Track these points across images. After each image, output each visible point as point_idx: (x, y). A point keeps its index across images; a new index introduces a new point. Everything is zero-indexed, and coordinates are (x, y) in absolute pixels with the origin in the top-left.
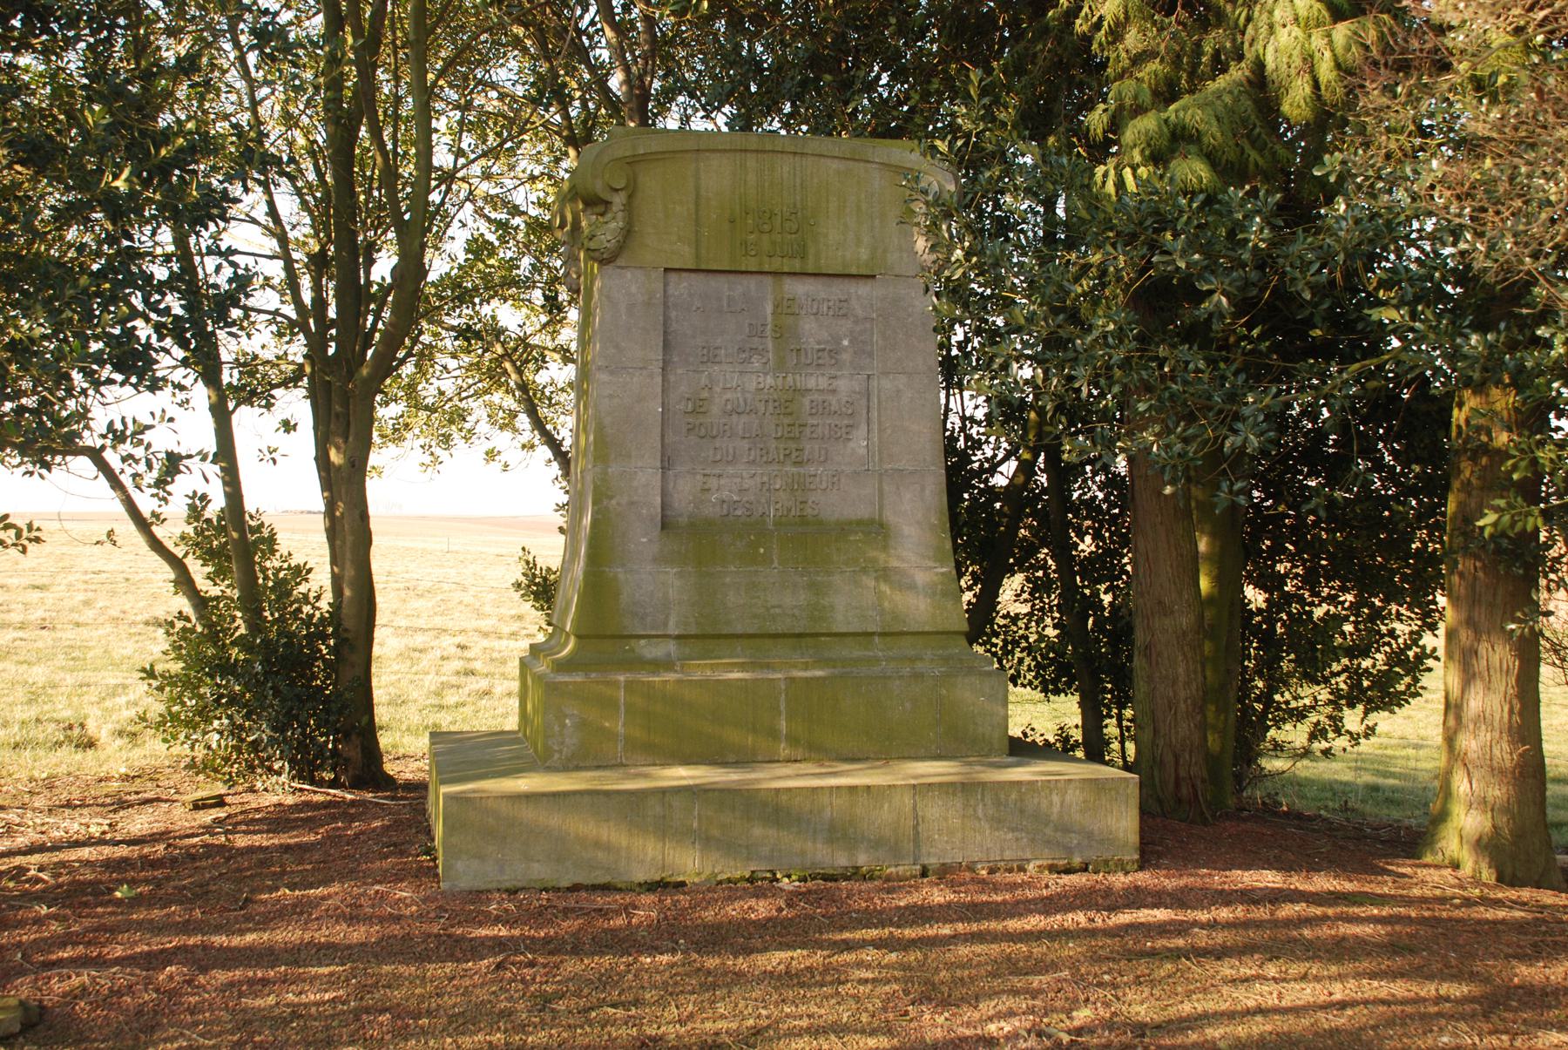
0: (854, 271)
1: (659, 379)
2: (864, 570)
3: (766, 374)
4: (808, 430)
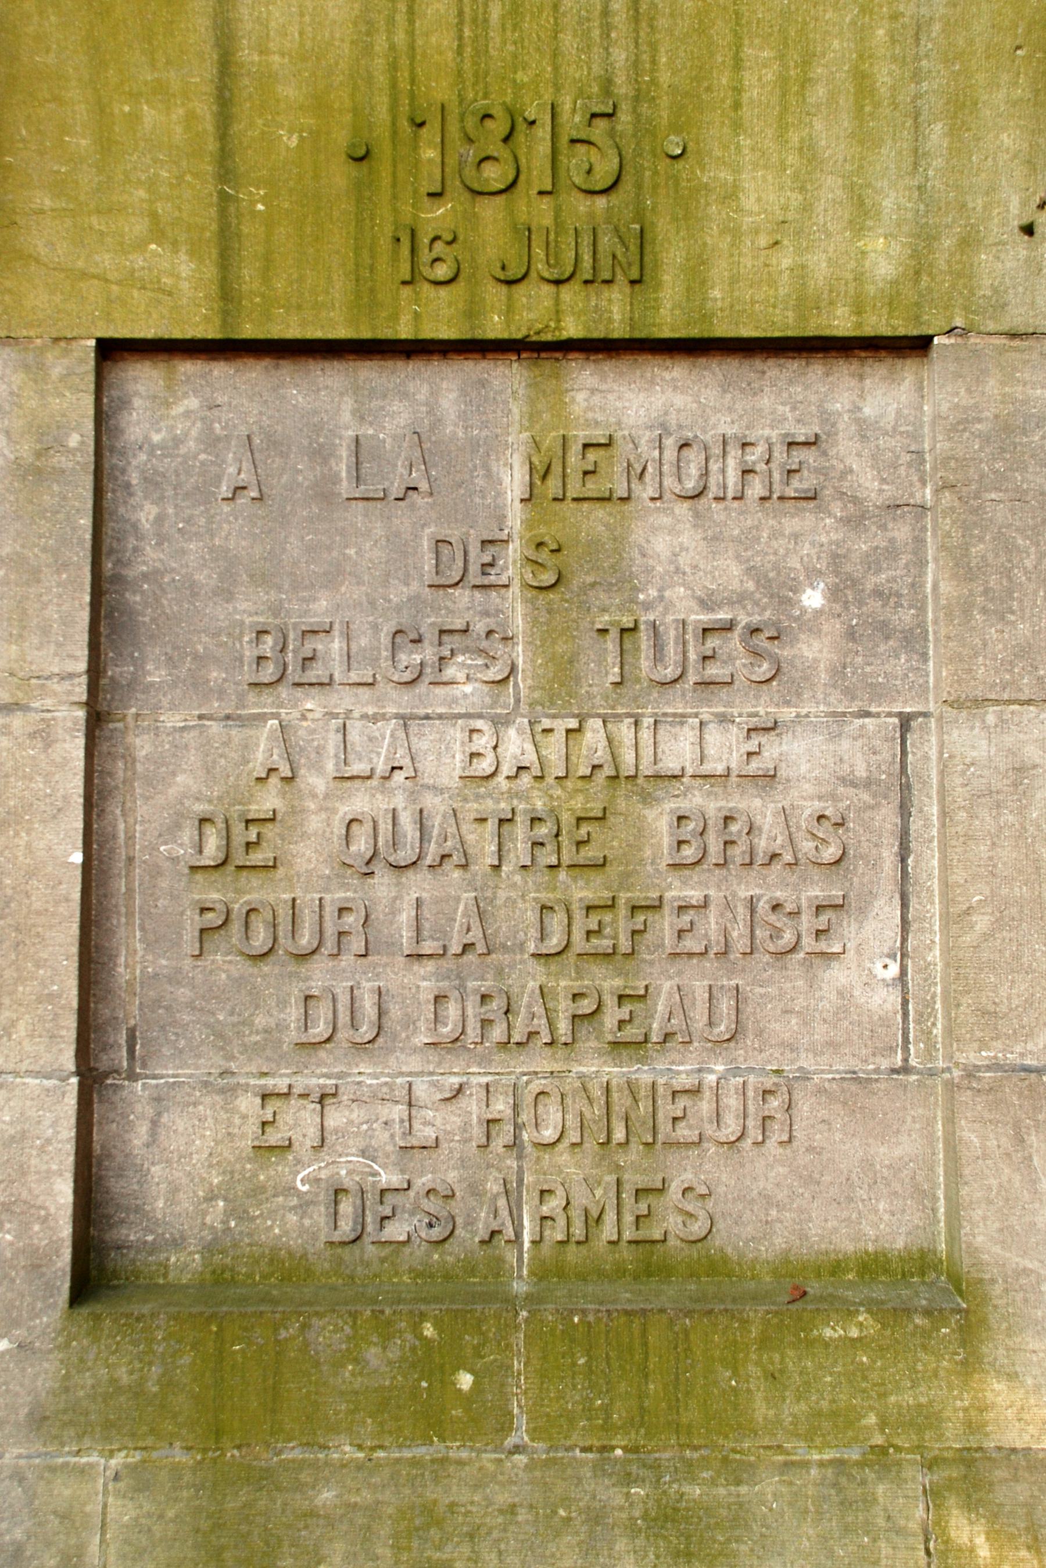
0: (841, 324)
1: (75, 748)
2: (881, 1458)
3: (500, 722)
4: (666, 924)
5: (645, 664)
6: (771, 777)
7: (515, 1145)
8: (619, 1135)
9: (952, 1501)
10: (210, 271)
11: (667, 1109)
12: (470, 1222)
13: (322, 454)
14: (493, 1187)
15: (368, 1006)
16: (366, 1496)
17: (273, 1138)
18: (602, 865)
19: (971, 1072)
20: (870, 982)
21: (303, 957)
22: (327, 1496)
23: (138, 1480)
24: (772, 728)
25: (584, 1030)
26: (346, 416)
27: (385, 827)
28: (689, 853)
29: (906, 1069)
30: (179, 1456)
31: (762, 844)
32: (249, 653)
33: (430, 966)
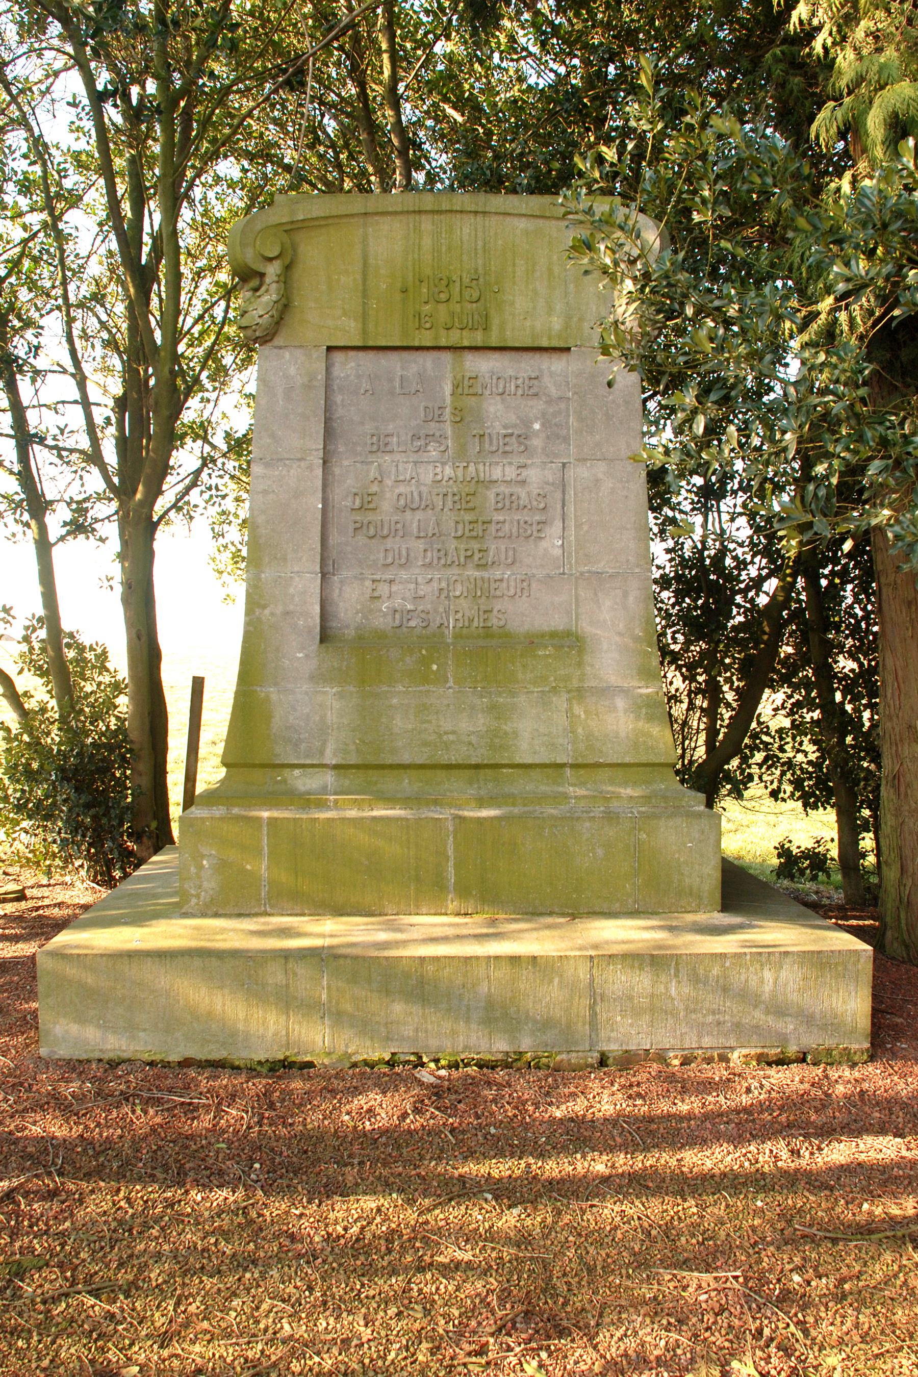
0: (545, 343)
1: (319, 472)
2: (554, 690)
3: (443, 464)
4: (493, 528)
5: (487, 446)
6: (524, 482)
7: (448, 597)
8: (479, 594)
9: (574, 702)
10: (360, 325)
11: (493, 586)
12: (434, 621)
13: (391, 380)
14: (441, 610)
15: (404, 553)
16: (406, 701)
17: (376, 594)
18: (473, 509)
19: (582, 574)
20: (553, 546)
21: (384, 537)
22: (395, 701)
23: (340, 696)
24: (525, 466)
25: (468, 560)
26: (398, 369)
27: (409, 496)
28: (500, 505)
29: (564, 574)
30: (352, 689)
31: (521, 502)
32: (369, 442)
33: (423, 540)
